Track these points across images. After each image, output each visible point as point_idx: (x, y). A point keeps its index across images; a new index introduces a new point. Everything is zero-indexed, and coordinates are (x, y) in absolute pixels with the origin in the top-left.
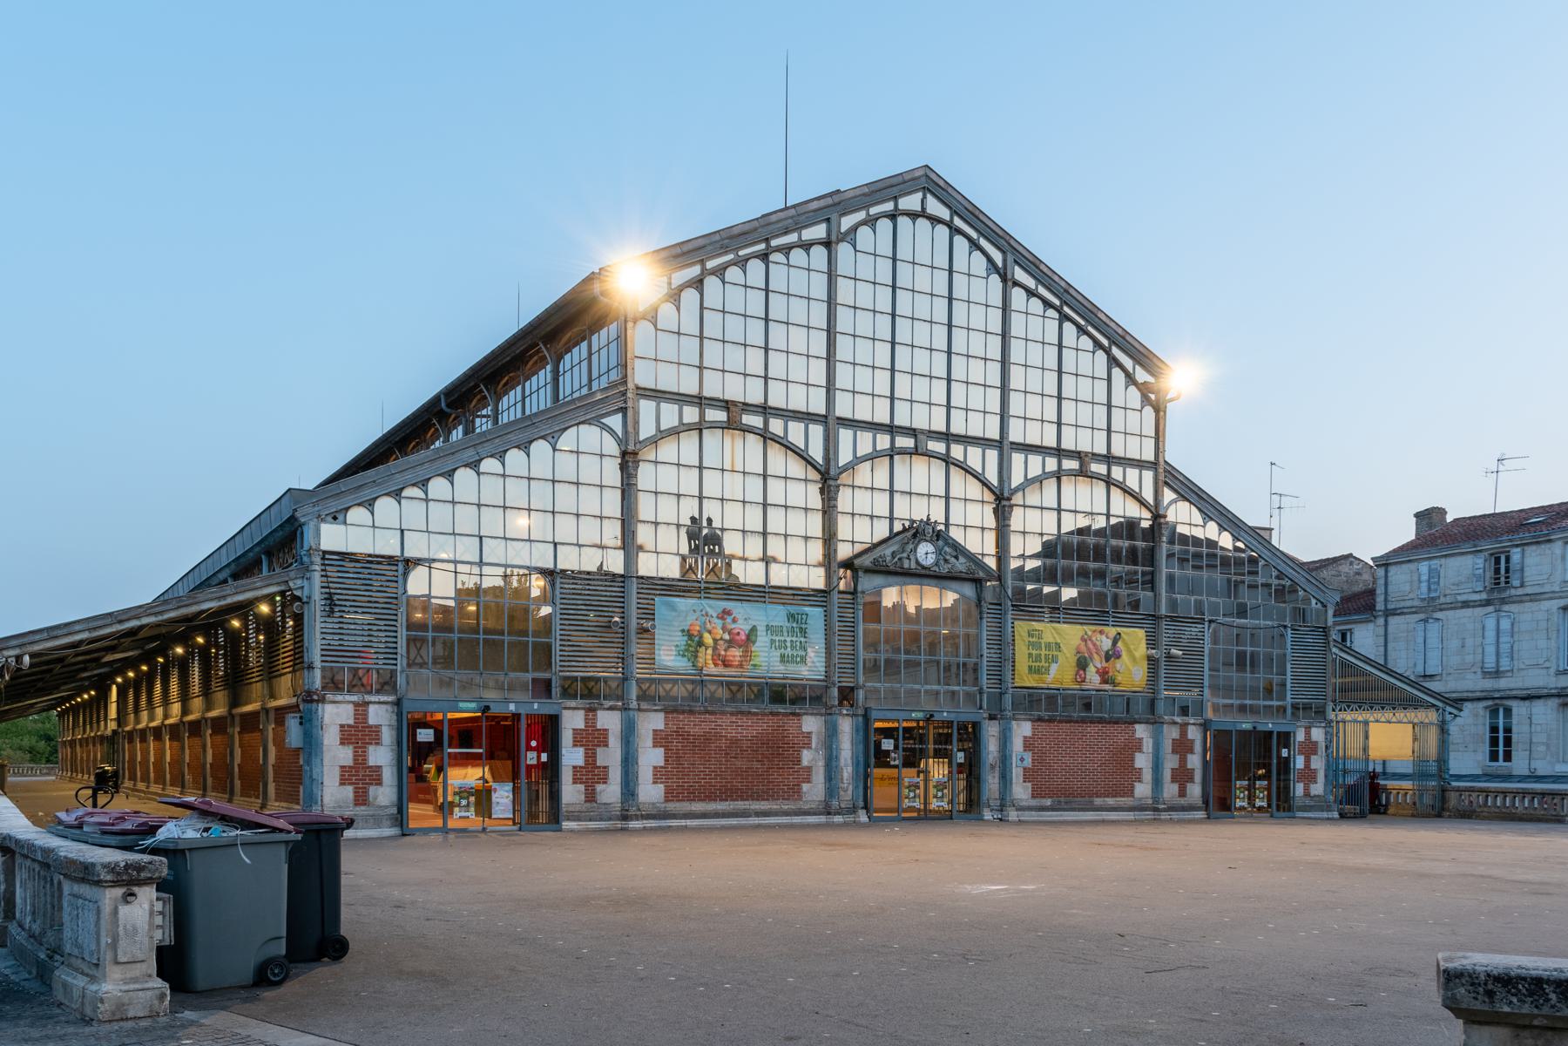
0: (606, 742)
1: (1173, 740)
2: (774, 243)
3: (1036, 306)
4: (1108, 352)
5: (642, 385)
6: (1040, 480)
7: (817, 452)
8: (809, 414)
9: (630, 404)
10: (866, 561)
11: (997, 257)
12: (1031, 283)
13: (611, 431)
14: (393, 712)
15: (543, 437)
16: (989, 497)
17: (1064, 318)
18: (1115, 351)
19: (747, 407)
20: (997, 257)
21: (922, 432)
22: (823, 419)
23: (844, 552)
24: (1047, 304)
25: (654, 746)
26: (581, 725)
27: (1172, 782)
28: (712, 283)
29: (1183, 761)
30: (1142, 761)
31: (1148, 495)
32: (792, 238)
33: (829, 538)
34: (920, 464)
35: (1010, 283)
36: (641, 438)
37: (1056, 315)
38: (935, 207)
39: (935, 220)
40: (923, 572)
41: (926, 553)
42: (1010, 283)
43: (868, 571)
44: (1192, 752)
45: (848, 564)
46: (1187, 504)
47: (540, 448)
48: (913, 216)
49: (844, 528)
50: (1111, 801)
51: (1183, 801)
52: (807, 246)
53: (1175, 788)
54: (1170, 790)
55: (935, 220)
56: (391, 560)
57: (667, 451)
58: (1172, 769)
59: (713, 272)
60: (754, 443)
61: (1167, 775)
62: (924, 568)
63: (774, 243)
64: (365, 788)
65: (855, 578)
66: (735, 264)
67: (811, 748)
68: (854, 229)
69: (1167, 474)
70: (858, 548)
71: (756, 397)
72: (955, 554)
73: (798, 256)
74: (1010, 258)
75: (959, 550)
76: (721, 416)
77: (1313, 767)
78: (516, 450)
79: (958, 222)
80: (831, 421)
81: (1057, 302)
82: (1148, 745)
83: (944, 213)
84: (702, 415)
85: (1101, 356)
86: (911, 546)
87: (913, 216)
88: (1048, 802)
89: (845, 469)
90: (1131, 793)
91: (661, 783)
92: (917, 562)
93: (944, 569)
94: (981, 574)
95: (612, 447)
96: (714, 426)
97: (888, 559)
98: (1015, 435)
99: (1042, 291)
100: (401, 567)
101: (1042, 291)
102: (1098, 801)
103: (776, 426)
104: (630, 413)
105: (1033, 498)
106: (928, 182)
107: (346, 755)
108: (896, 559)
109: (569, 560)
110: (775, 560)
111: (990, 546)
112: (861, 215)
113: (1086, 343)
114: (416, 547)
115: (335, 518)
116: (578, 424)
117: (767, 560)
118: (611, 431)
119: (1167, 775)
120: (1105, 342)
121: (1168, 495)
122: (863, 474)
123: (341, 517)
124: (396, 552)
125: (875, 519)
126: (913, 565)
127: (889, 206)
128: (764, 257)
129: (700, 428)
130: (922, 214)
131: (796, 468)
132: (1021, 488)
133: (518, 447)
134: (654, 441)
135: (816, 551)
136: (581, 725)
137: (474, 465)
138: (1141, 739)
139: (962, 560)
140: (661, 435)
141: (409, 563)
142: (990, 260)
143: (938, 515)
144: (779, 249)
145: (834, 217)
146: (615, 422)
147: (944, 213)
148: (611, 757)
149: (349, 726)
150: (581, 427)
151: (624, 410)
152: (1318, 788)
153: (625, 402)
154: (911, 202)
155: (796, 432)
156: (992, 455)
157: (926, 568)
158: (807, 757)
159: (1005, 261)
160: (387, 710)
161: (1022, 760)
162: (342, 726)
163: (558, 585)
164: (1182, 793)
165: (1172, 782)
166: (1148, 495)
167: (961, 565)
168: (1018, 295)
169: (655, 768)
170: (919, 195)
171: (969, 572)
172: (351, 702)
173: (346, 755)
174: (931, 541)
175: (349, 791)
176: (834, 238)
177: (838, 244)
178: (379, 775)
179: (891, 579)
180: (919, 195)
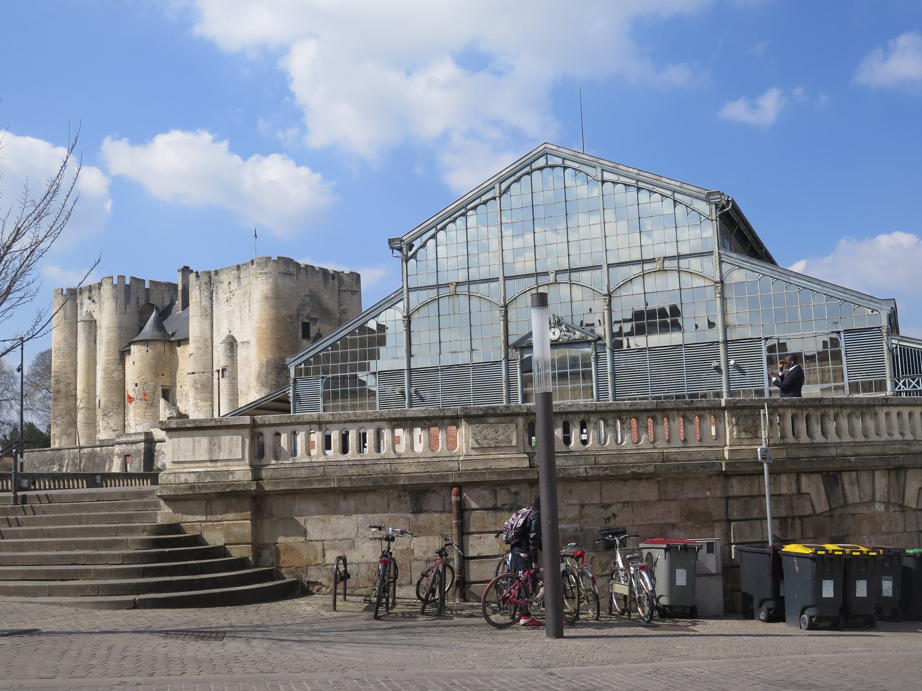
2: (469, 207)
12: (614, 177)
39: (553, 167)
48: (541, 169)
63: (469, 207)
68: (509, 187)
79: (567, 163)
99: (622, 179)
101: (622, 179)
112: (513, 179)
127: (527, 169)
130: (547, 166)
144: (471, 209)
150: (387, 310)
154: (541, 162)
177: (500, 197)
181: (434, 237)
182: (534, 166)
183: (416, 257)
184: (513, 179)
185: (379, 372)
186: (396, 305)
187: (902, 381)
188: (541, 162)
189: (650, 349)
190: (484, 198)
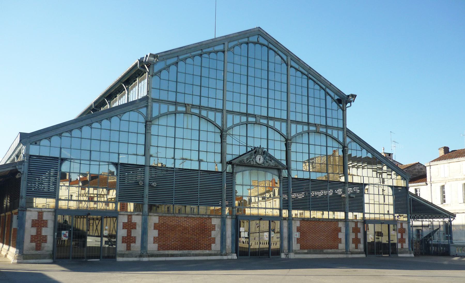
0: (135, 227)
1: (353, 228)
2: (204, 51)
3: (299, 74)
4: (325, 90)
5: (154, 98)
6: (301, 134)
7: (219, 123)
8: (216, 109)
9: (149, 104)
10: (237, 161)
11: (285, 57)
12: (297, 66)
13: (142, 114)
14: (53, 215)
15: (116, 116)
16: (283, 139)
17: (309, 78)
18: (328, 90)
19: (193, 106)
20: (285, 57)
21: (258, 116)
22: (222, 111)
23: (229, 158)
24: (302, 73)
25: (154, 229)
26: (126, 221)
27: (353, 243)
28: (181, 64)
29: (356, 235)
30: (342, 236)
31: (341, 140)
32: (211, 49)
33: (222, 153)
34: (257, 128)
35: (289, 66)
36: (153, 116)
37: (306, 77)
38: (262, 40)
39: (263, 45)
40: (258, 166)
41: (260, 159)
42: (289, 66)
43: (237, 165)
44: (359, 232)
45: (230, 163)
46: (355, 143)
47: (115, 120)
48: (255, 43)
49: (229, 150)
50: (330, 251)
51: (356, 250)
52: (216, 52)
53: (353, 246)
54: (352, 246)
55: (263, 45)
56: (56, 159)
57: (163, 121)
58: (353, 238)
59: (182, 60)
60: (196, 119)
61: (351, 241)
62: (258, 164)
64: (40, 244)
65: (233, 168)
66: (190, 58)
67: (215, 230)
69: (347, 132)
70: (234, 157)
71: (196, 103)
72: (270, 159)
73: (213, 55)
74: (289, 58)
75: (272, 158)
76: (183, 109)
77: (404, 237)
78: (106, 120)
79: (271, 46)
80: (225, 112)
81: (306, 73)
82: (343, 230)
83: (266, 43)
84: (176, 109)
85: (323, 92)
86: (253, 156)
87: (255, 43)
88: (306, 251)
89: (230, 128)
90: (337, 248)
91: (157, 243)
92: (256, 162)
93: (266, 165)
94: (280, 167)
95: (142, 120)
96: (180, 112)
97: (245, 161)
98: (292, 117)
99: (301, 69)
100: (59, 161)
102: (325, 251)
103: (204, 113)
104: (149, 107)
105: (299, 140)
106: (259, 32)
107: (33, 231)
108: (248, 161)
109: (123, 159)
110: (202, 161)
111: (284, 157)
112: (236, 43)
113: (317, 87)
114: (66, 154)
115: (36, 143)
116: (129, 111)
117: (200, 161)
118: (142, 114)
119: (351, 241)
120: (324, 87)
121: (348, 140)
122: (236, 131)
123: (38, 143)
124: (58, 156)
125: (240, 146)
126: (255, 163)
127: (246, 40)
128: (201, 55)
129: (175, 113)
131: (211, 128)
132: (295, 136)
133: (107, 119)
134: (158, 117)
135: (218, 158)
136: (126, 221)
137: (90, 125)
138: (341, 227)
139: (273, 161)
140: (161, 116)
141: (63, 160)
142: (282, 58)
143: (264, 145)
144: (206, 53)
145: (226, 43)
146: (144, 110)
147: (266, 43)
148: (137, 233)
149: (36, 220)
150: (131, 112)
151: (147, 107)
152: (406, 245)
153: (147, 103)
155: (211, 115)
156: (284, 125)
157: (260, 164)
158: (213, 233)
159: (287, 59)
160: (50, 214)
161: (296, 235)
162: (33, 220)
163: (119, 169)
164: (357, 247)
165: (353, 243)
166: (341, 140)
167: (272, 163)
168: (292, 71)
169: (154, 237)
170: (257, 36)
171: (276, 166)
172: (37, 211)
173: (33, 231)
174: (261, 155)
175: (34, 244)
176: (226, 50)
178: (46, 239)
179: (247, 168)
180: (257, 36)
181: (176, 64)
182: (251, 39)
183: (160, 75)
184: (236, 43)
185: (121, 164)
186: (140, 110)
187: (412, 216)
188: (254, 39)
189: (312, 180)
190: (217, 48)
